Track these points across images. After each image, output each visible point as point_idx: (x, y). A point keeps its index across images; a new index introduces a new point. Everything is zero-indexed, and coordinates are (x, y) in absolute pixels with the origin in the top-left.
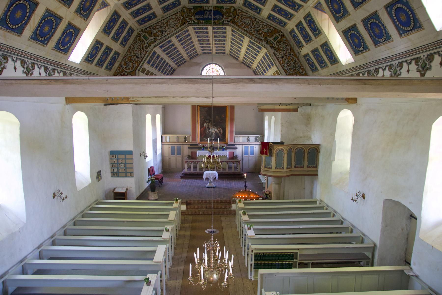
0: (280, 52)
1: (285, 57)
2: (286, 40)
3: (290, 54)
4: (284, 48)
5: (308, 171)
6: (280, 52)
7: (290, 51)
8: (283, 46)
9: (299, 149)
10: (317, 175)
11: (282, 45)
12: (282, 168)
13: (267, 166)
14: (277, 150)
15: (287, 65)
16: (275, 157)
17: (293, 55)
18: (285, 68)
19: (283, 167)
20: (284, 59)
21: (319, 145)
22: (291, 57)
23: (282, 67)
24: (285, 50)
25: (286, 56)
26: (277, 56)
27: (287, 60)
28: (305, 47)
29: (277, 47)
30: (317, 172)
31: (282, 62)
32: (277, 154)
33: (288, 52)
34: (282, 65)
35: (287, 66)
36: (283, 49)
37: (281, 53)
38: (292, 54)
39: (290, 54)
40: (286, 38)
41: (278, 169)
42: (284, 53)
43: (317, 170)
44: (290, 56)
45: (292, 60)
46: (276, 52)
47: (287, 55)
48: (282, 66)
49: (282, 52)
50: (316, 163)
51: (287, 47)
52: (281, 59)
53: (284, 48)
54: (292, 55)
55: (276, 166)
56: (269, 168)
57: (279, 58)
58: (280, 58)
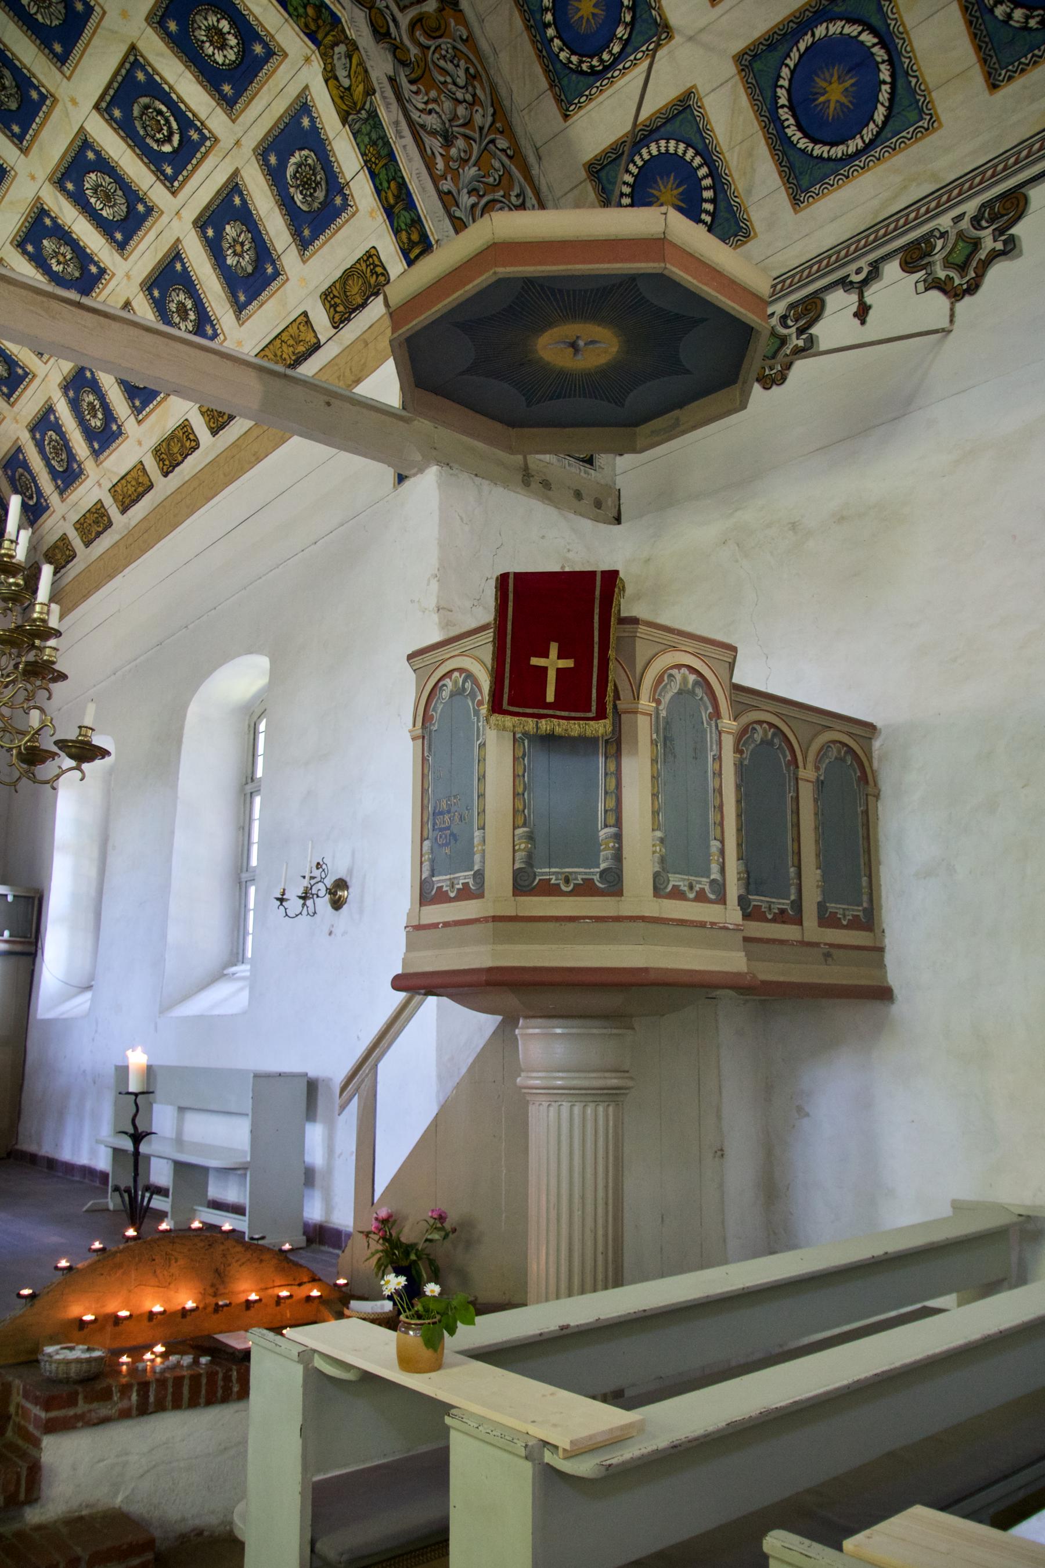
0: (433, 94)
1: (460, 143)
2: (469, 40)
3: (493, 141)
4: (454, 83)
5: (829, 953)
6: (433, 94)
7: (490, 119)
8: (449, 67)
9: (758, 737)
10: (884, 994)
11: (444, 57)
12: (703, 884)
13: (544, 872)
14: (660, 680)
15: (473, 199)
16: (654, 761)
17: (510, 157)
18: (458, 214)
19: (715, 875)
20: (453, 151)
21: (871, 727)
22: (497, 164)
23: (441, 199)
24: (459, 95)
25: (467, 137)
26: (415, 115)
27: (473, 171)
28: (678, 39)
29: (414, 51)
30: (881, 965)
31: (440, 164)
32: (668, 723)
33: (478, 119)
34: (446, 185)
35: (473, 206)
36: (454, 88)
37: (435, 101)
38: (502, 143)
39: (493, 141)
40: (466, 25)
41: (677, 894)
42: (455, 117)
43: (881, 950)
44: (494, 156)
45: (504, 181)
46: (404, 81)
47: (477, 136)
48: (441, 194)
49: (447, 105)
50: (864, 880)
51: (474, 88)
52: (434, 144)
53: (454, 83)
54: (503, 150)
55: (663, 860)
56: (587, 889)
57: (423, 126)
58: (433, 133)
